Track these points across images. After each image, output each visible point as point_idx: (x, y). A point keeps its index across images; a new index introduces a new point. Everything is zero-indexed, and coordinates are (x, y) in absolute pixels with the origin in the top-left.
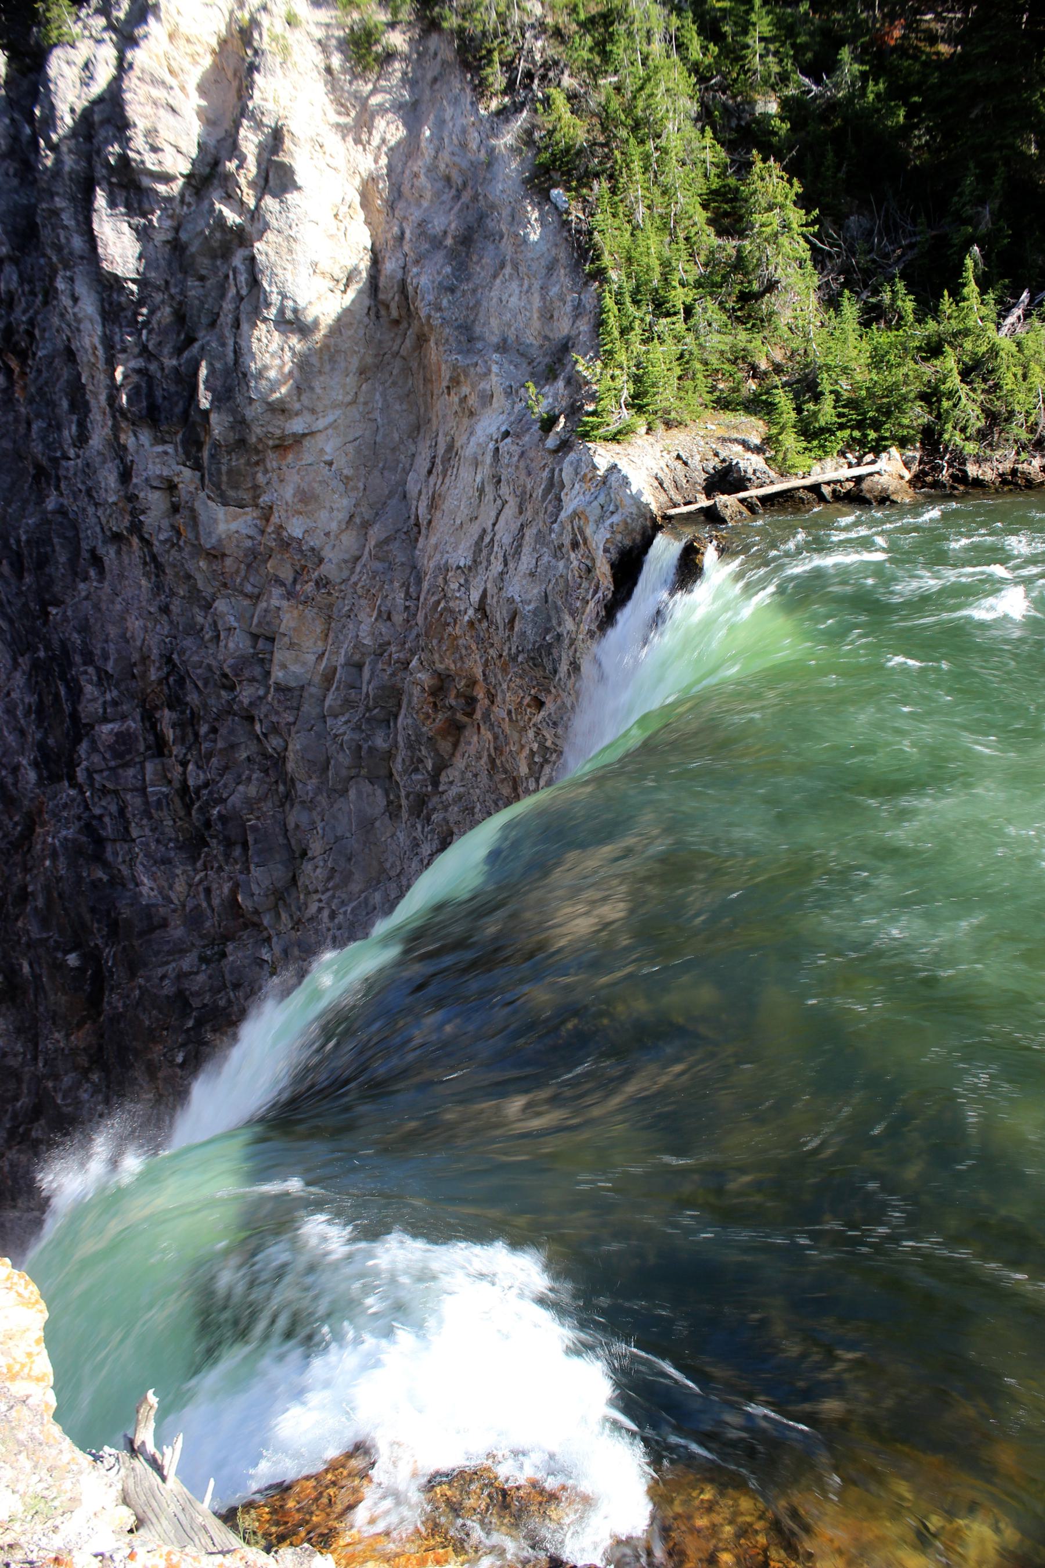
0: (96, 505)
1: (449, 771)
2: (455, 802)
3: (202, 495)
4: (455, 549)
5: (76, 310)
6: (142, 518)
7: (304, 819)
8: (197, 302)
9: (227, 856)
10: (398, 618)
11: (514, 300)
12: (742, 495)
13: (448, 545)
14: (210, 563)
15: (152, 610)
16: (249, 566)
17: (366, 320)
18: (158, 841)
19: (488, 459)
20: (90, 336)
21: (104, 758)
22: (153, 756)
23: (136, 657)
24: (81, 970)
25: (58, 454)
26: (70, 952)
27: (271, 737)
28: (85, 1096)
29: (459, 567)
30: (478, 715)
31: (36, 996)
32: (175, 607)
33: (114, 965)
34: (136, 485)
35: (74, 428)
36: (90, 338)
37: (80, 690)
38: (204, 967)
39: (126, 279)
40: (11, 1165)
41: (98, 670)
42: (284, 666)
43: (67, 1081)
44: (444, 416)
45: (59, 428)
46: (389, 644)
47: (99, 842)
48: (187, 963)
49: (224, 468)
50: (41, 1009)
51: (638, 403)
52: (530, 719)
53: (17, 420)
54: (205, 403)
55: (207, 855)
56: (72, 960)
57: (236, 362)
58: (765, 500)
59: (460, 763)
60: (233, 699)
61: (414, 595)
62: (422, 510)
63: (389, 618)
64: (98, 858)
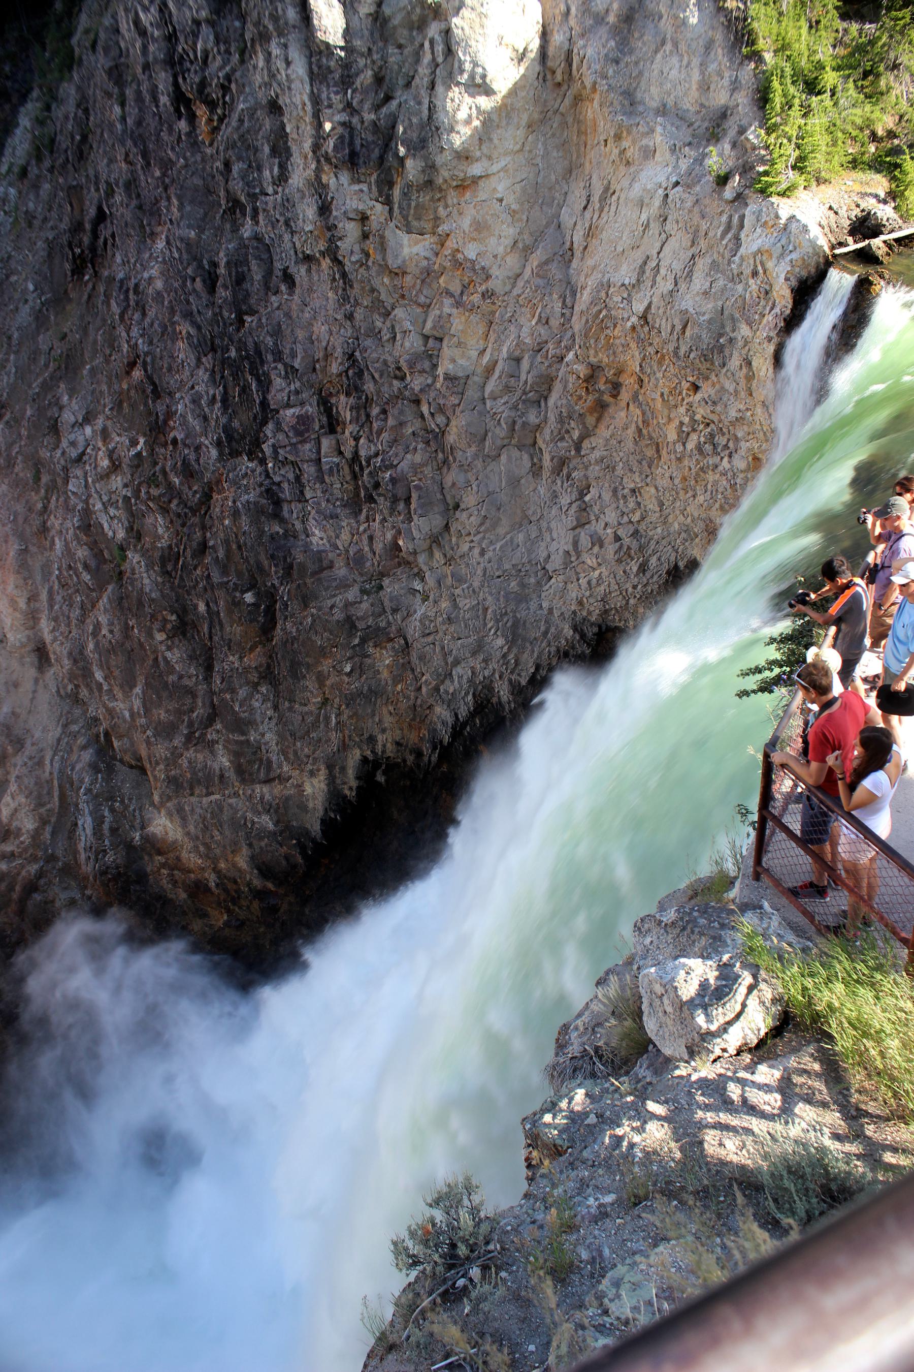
0: (293, 233)
1: (592, 439)
2: (597, 462)
3: (392, 225)
4: (617, 269)
5: (289, 72)
6: (339, 243)
7: (461, 479)
8: (396, 67)
9: (392, 510)
10: (555, 322)
11: (674, 73)
12: (883, 237)
14: (392, 279)
15: (339, 317)
16: (423, 281)
17: (536, 83)
18: (328, 501)
19: (657, 202)
20: (300, 94)
21: (287, 436)
22: (326, 434)
23: (320, 355)
24: (256, 605)
25: (257, 191)
27: (437, 416)
28: (256, 704)
29: (623, 285)
30: (625, 395)
32: (359, 314)
33: (289, 599)
34: (336, 217)
35: (276, 169)
36: (298, 97)
37: (270, 382)
38: (365, 598)
39: (335, 47)
40: (190, 762)
41: (286, 365)
42: (453, 361)
43: (242, 693)
44: (599, 163)
45: (259, 169)
46: (546, 342)
47: (278, 503)
48: (352, 594)
49: (413, 204)
50: (216, 638)
51: (799, 166)
52: (683, 399)
53: (203, 160)
54: (402, 151)
55: (370, 509)
56: (249, 597)
57: (430, 117)
58: (897, 240)
59: (604, 432)
60: (405, 387)
61: (569, 305)
62: (578, 238)
63: (547, 323)
64: (277, 516)
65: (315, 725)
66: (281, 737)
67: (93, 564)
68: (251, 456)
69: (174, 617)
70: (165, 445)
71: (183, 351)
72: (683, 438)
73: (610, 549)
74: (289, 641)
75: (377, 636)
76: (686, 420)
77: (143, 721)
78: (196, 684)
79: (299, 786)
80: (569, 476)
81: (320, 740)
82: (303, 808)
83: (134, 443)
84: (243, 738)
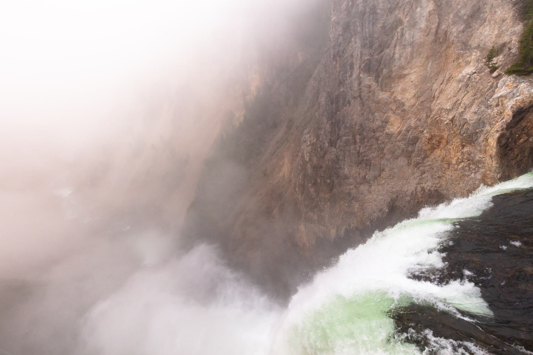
4: (446, 104)
7: (386, 163)
10: (422, 121)
13: (444, 102)
23: (354, 124)
24: (329, 184)
32: (365, 114)
42: (389, 129)
43: (323, 203)
45: (346, 73)
48: (352, 187)
57: (393, 56)
59: (432, 157)
68: (335, 147)
71: (325, 120)
72: (458, 163)
76: (460, 157)
80: (419, 168)
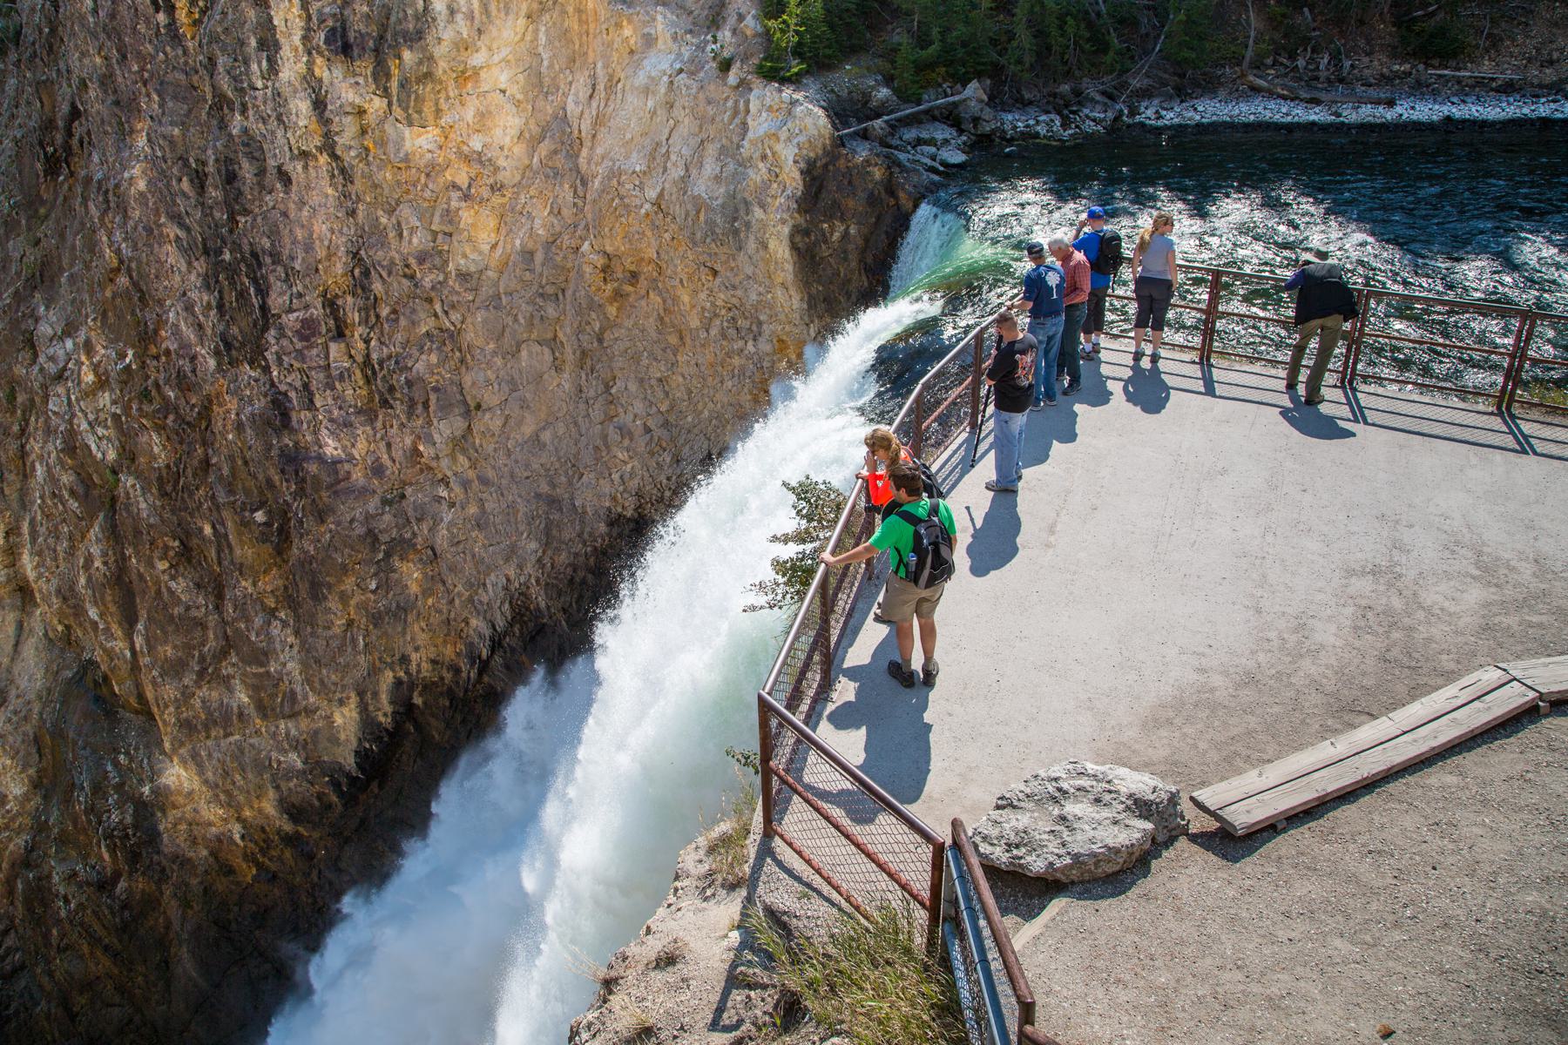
4: (627, 157)
9: (410, 414)
14: (394, 174)
24: (267, 524)
26: (256, 510)
28: (275, 632)
31: (218, 553)
35: (264, 63)
37: (269, 287)
42: (465, 256)
43: (258, 621)
45: (246, 62)
47: (285, 416)
48: (373, 504)
56: (260, 516)
65: (341, 649)
66: (305, 666)
67: (80, 490)
69: (177, 543)
70: (157, 358)
71: (171, 255)
73: (641, 443)
74: (307, 560)
75: (402, 547)
77: (147, 660)
78: (206, 615)
79: (329, 718)
81: (348, 665)
82: (334, 740)
83: (122, 356)
84: (262, 670)
